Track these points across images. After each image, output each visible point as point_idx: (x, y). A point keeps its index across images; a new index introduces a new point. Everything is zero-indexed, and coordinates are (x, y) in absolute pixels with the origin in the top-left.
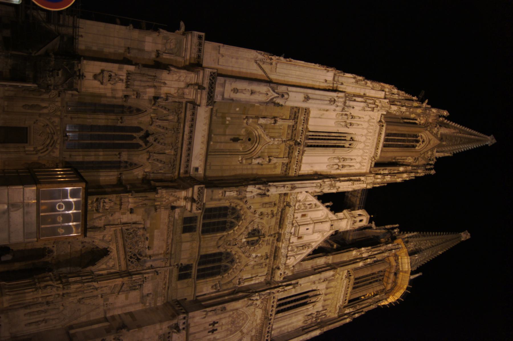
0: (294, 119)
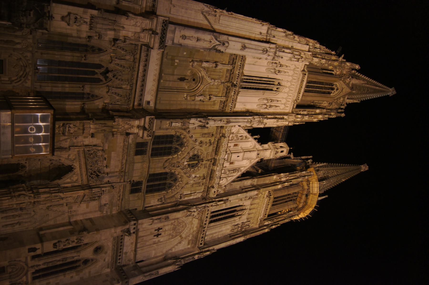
0: (232, 65)
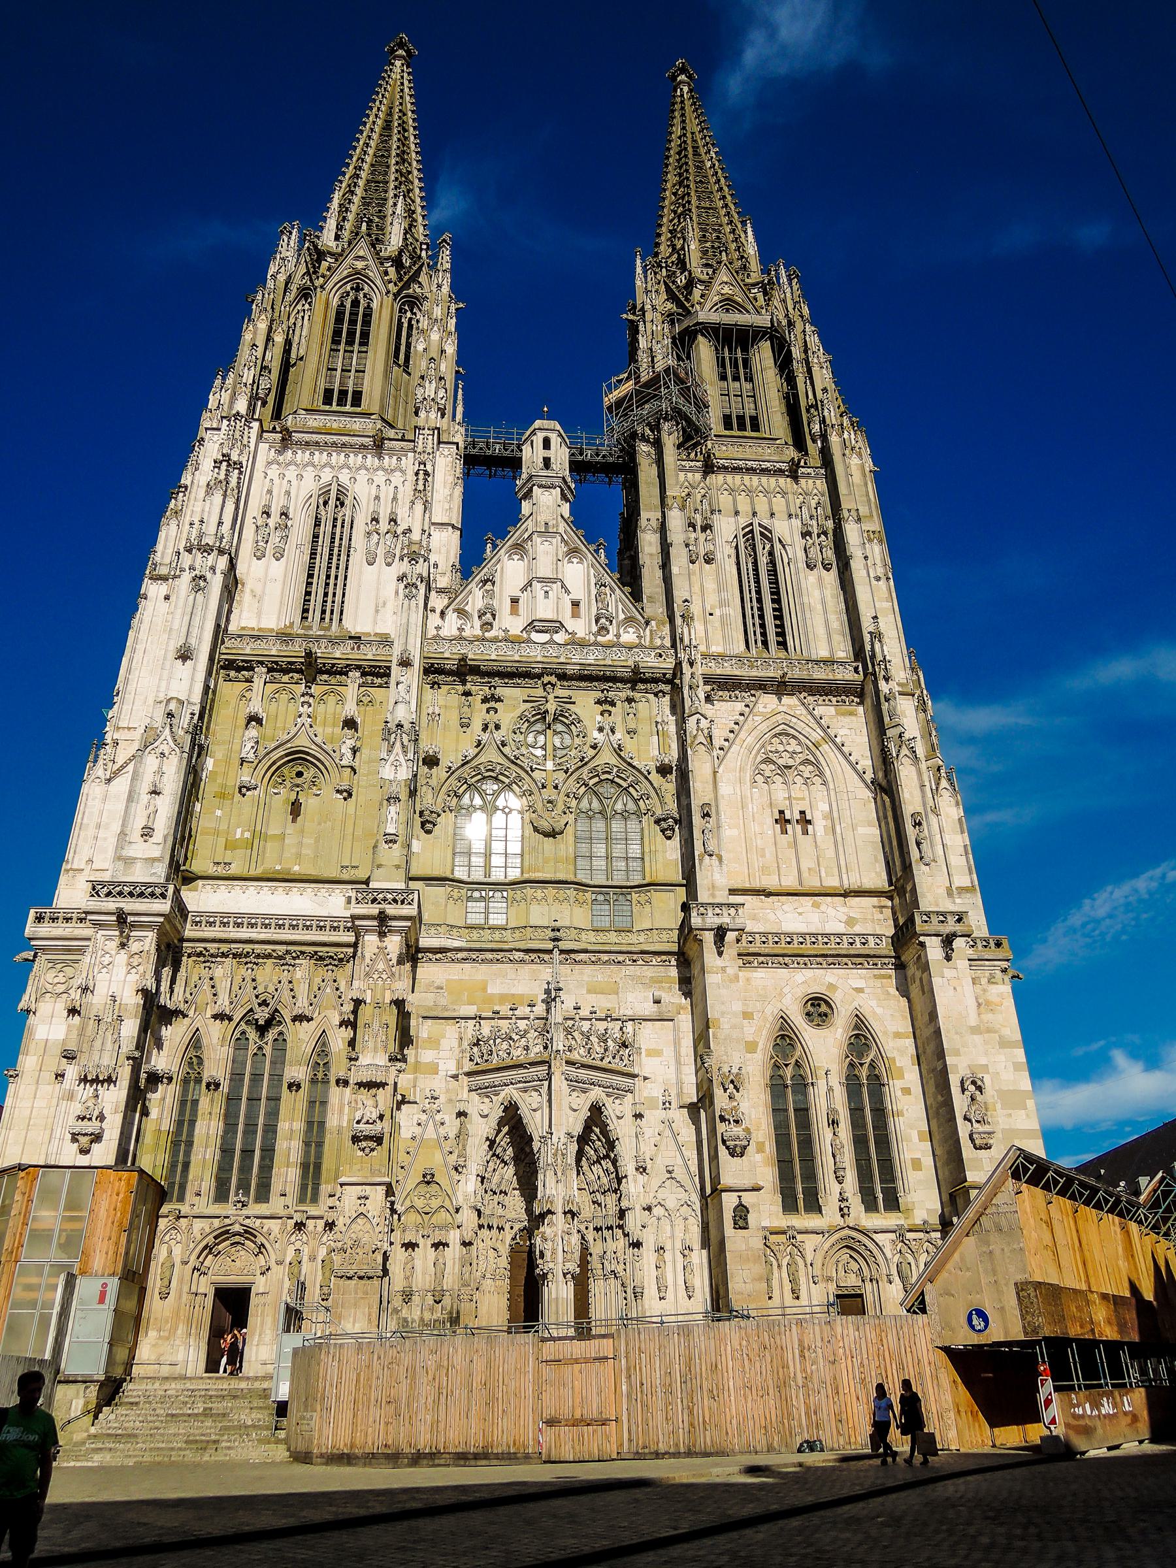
0: (252, 669)
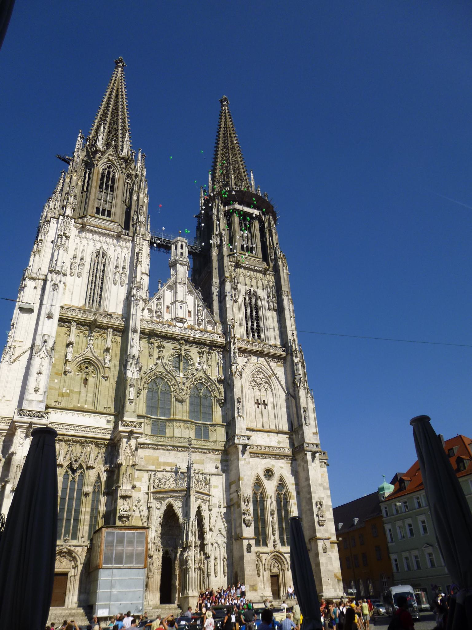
0: (70, 323)
